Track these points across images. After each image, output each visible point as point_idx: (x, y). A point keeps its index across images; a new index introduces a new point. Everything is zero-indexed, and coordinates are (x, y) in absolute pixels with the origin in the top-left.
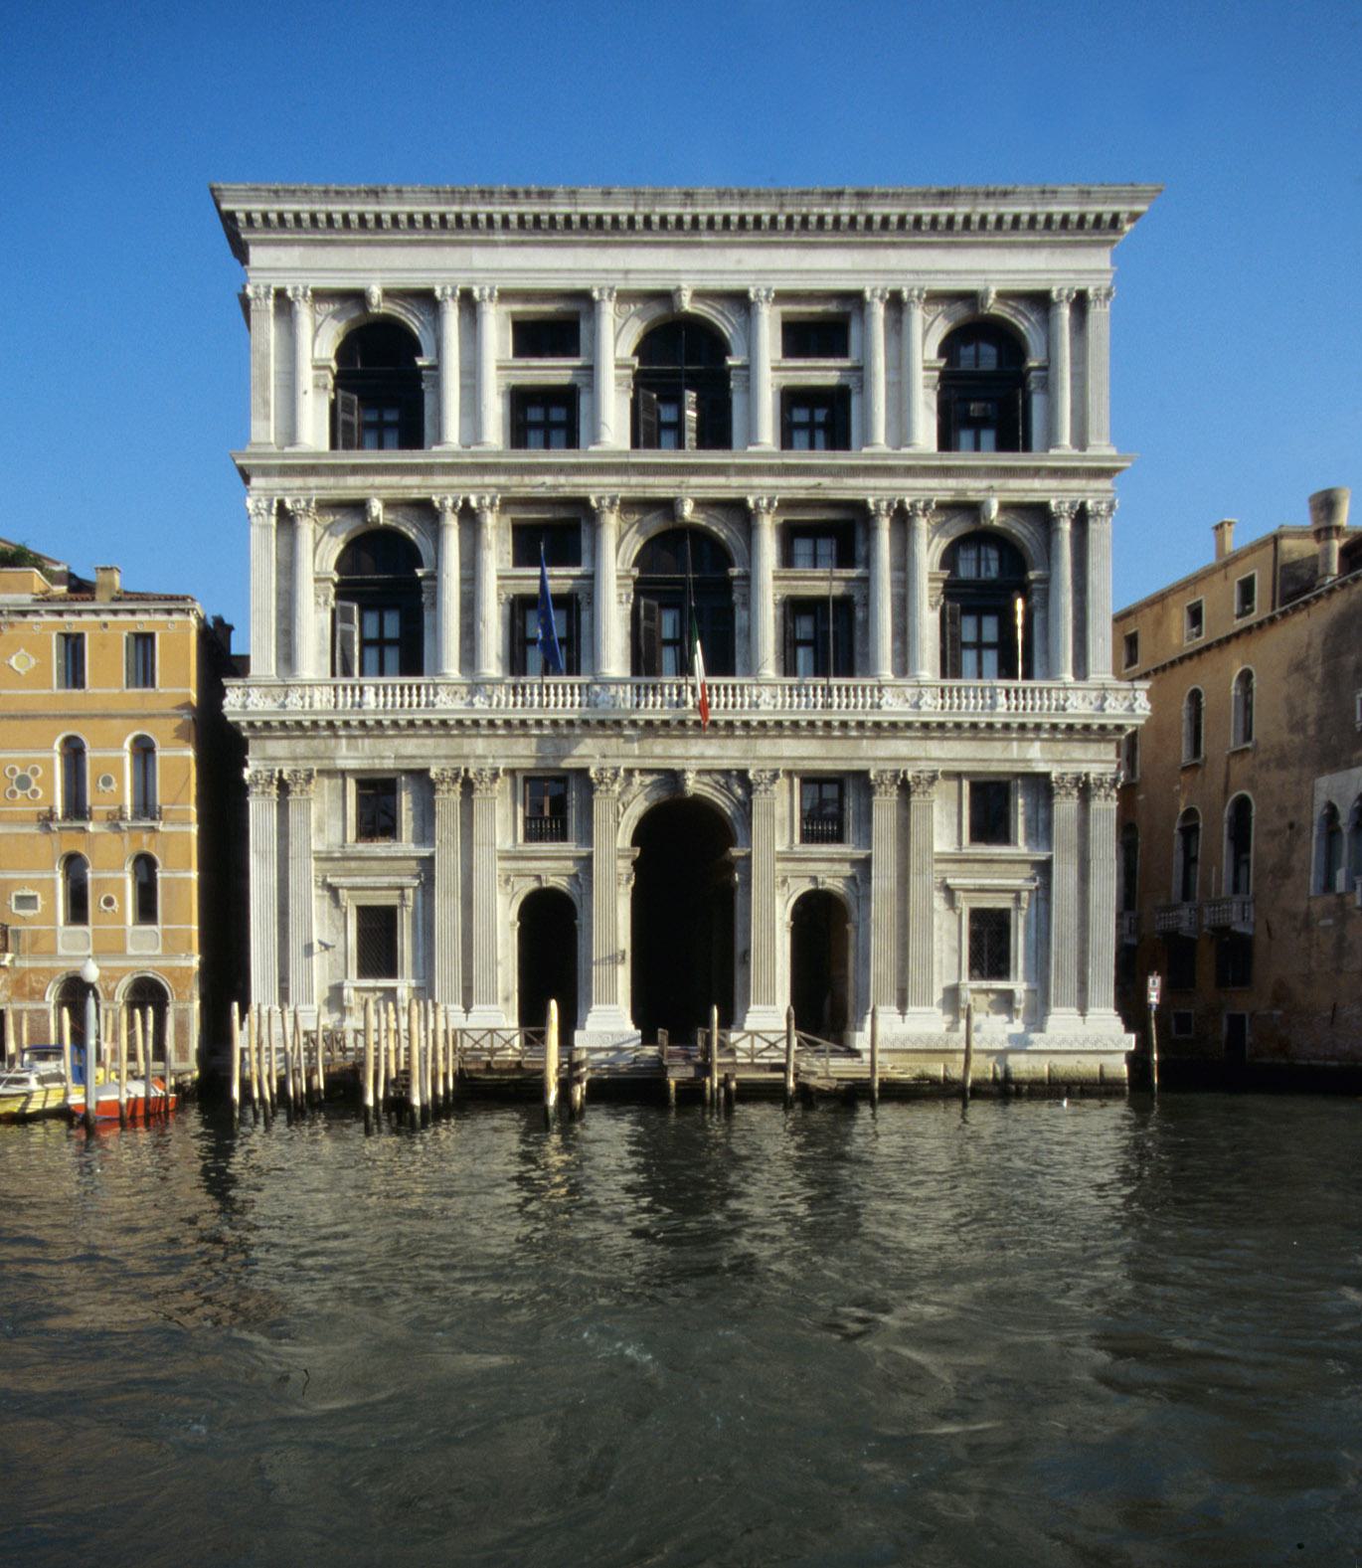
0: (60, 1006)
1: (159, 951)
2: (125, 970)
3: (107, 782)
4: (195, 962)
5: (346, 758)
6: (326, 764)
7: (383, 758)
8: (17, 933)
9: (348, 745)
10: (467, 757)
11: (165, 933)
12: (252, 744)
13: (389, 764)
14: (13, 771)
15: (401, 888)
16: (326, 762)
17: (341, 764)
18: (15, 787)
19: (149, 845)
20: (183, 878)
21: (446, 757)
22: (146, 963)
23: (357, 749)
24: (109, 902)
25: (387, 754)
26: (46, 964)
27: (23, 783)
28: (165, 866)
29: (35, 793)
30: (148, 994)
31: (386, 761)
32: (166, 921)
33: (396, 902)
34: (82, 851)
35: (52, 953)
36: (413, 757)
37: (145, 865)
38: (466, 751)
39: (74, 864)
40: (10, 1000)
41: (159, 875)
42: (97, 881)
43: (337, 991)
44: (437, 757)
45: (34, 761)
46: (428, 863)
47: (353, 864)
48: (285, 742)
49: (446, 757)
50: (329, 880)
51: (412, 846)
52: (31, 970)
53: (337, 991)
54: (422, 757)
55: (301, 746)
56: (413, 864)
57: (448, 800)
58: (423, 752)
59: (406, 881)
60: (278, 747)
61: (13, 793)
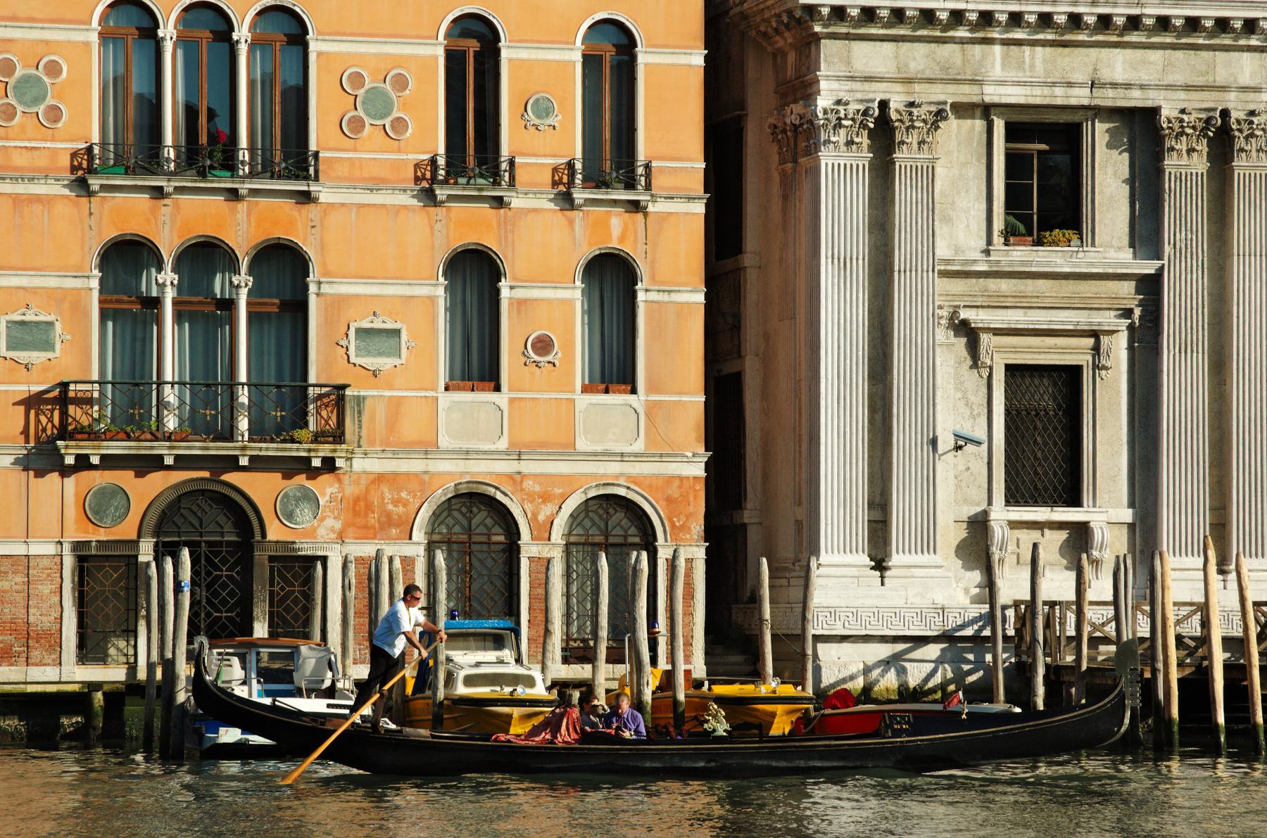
0: (430, 548)
1: (639, 446)
2: (570, 482)
3: (544, 110)
4: (698, 470)
5: (1002, 83)
6: (967, 94)
7: (1070, 84)
8: (360, 400)
9: (1005, 57)
10: (1224, 88)
11: (651, 409)
12: (828, 49)
13: (1080, 96)
14: (357, 79)
15: (1095, 334)
16: (966, 89)
17: (993, 94)
18: (360, 112)
19: (622, 239)
20: (673, 302)
21: (1188, 88)
22: (614, 468)
23: (1020, 66)
24: (543, 345)
25: (1078, 77)
26: (414, 465)
27: (379, 104)
28: (653, 279)
29: (400, 124)
30: (616, 524)
31: (1076, 91)
32: (651, 389)
33: (1084, 359)
34: (490, 242)
35: (429, 448)
36: (1128, 86)
37: (612, 277)
38: (1221, 77)
39: (475, 273)
40: (341, 539)
41: (641, 296)
42: (521, 304)
43: (979, 525)
44: (1170, 87)
45: (399, 60)
46: (1151, 286)
47: (1004, 285)
48: (888, 47)
49: (1188, 88)
50: (964, 314)
51: (1127, 255)
52: (380, 478)
53: (979, 525)
54: (1142, 87)
55: (919, 57)
56: (1128, 288)
57: (1186, 165)
58: (1145, 77)
59: (1107, 319)
60: (874, 57)
61: (357, 124)
